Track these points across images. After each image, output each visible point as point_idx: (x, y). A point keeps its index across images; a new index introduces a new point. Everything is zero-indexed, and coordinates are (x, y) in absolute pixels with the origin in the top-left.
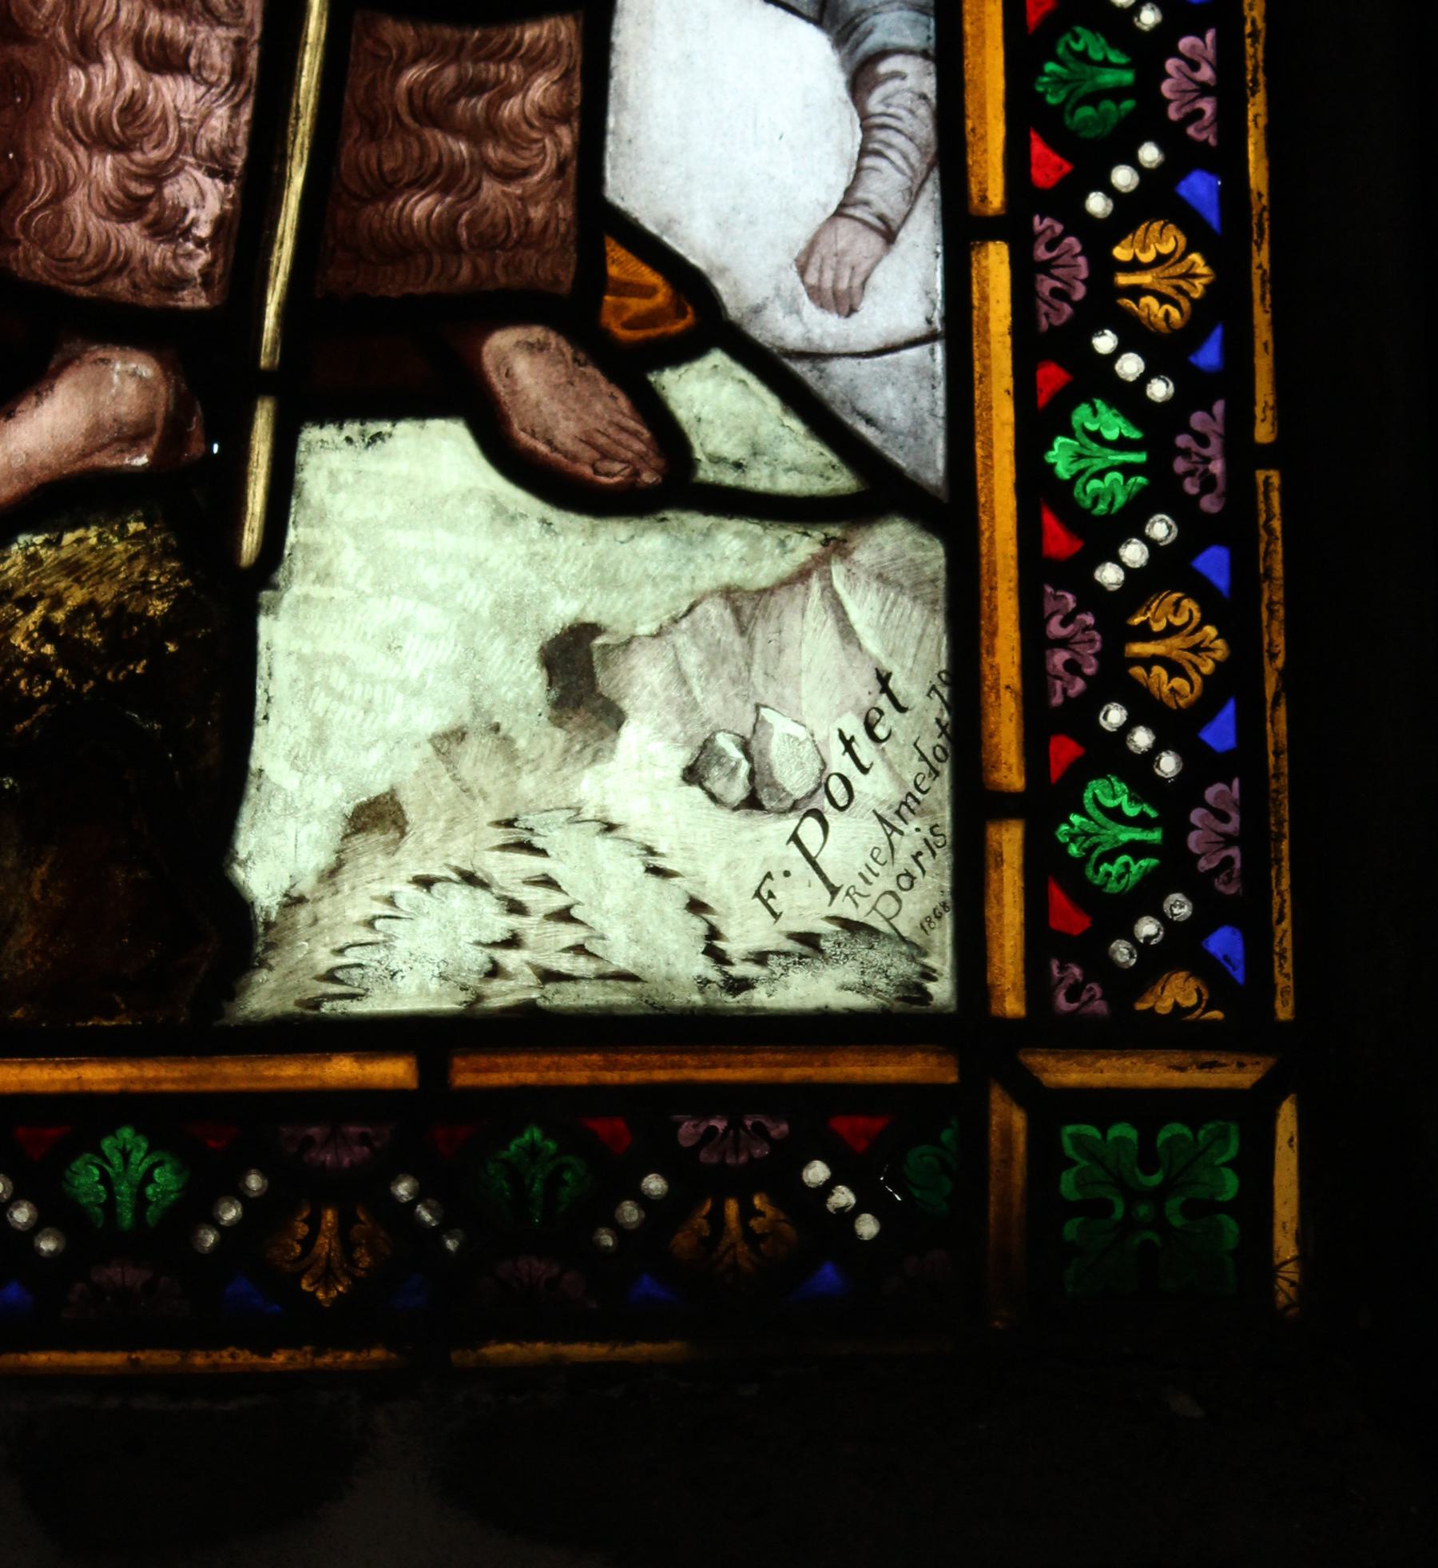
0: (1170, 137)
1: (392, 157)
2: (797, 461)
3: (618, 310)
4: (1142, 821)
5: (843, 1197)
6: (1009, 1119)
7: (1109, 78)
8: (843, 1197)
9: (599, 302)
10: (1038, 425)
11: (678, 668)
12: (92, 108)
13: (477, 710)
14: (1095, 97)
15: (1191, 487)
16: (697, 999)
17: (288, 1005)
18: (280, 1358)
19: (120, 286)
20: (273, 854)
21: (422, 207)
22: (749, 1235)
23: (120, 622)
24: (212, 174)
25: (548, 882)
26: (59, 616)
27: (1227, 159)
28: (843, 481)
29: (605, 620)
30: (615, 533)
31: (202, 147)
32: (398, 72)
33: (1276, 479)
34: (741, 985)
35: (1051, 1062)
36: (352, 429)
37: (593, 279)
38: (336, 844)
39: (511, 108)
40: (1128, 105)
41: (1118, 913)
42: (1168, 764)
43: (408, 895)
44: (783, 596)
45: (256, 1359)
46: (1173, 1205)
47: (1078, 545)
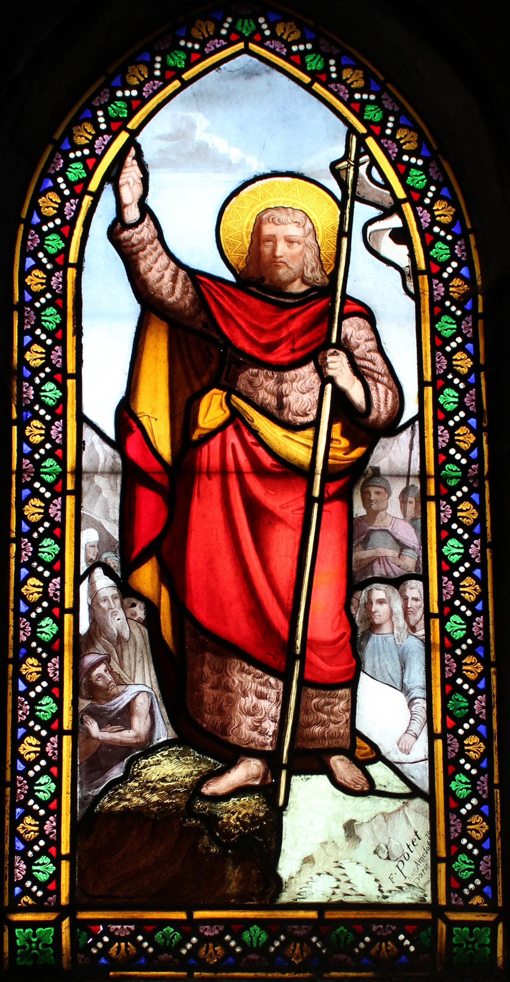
0: (476, 717)
1: (311, 718)
2: (399, 787)
3: (359, 752)
4: (470, 864)
5: (407, 942)
6: (442, 926)
7: (463, 704)
8: (407, 942)
9: (355, 751)
10: (448, 778)
11: (372, 829)
12: (246, 707)
13: (330, 838)
14: (460, 709)
15: (480, 793)
16: (377, 900)
17: (290, 900)
18: (287, 975)
19: (253, 745)
20: (286, 867)
21: (317, 729)
22: (387, 951)
23: (253, 817)
24: (272, 721)
25: (345, 875)
26: (240, 816)
27: (488, 723)
28: (407, 790)
29: (357, 819)
30: (359, 800)
31: (270, 716)
32: (312, 700)
33: (498, 791)
34: (385, 897)
35: (451, 914)
36: (303, 777)
37: (353, 745)
38: (300, 866)
39: (336, 708)
40: (467, 710)
41: (465, 883)
42: (476, 852)
43: (316, 877)
44: (394, 814)
45: (282, 975)
46: (476, 945)
47: (457, 805)
